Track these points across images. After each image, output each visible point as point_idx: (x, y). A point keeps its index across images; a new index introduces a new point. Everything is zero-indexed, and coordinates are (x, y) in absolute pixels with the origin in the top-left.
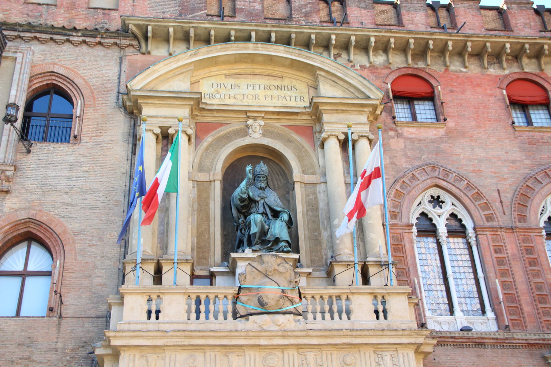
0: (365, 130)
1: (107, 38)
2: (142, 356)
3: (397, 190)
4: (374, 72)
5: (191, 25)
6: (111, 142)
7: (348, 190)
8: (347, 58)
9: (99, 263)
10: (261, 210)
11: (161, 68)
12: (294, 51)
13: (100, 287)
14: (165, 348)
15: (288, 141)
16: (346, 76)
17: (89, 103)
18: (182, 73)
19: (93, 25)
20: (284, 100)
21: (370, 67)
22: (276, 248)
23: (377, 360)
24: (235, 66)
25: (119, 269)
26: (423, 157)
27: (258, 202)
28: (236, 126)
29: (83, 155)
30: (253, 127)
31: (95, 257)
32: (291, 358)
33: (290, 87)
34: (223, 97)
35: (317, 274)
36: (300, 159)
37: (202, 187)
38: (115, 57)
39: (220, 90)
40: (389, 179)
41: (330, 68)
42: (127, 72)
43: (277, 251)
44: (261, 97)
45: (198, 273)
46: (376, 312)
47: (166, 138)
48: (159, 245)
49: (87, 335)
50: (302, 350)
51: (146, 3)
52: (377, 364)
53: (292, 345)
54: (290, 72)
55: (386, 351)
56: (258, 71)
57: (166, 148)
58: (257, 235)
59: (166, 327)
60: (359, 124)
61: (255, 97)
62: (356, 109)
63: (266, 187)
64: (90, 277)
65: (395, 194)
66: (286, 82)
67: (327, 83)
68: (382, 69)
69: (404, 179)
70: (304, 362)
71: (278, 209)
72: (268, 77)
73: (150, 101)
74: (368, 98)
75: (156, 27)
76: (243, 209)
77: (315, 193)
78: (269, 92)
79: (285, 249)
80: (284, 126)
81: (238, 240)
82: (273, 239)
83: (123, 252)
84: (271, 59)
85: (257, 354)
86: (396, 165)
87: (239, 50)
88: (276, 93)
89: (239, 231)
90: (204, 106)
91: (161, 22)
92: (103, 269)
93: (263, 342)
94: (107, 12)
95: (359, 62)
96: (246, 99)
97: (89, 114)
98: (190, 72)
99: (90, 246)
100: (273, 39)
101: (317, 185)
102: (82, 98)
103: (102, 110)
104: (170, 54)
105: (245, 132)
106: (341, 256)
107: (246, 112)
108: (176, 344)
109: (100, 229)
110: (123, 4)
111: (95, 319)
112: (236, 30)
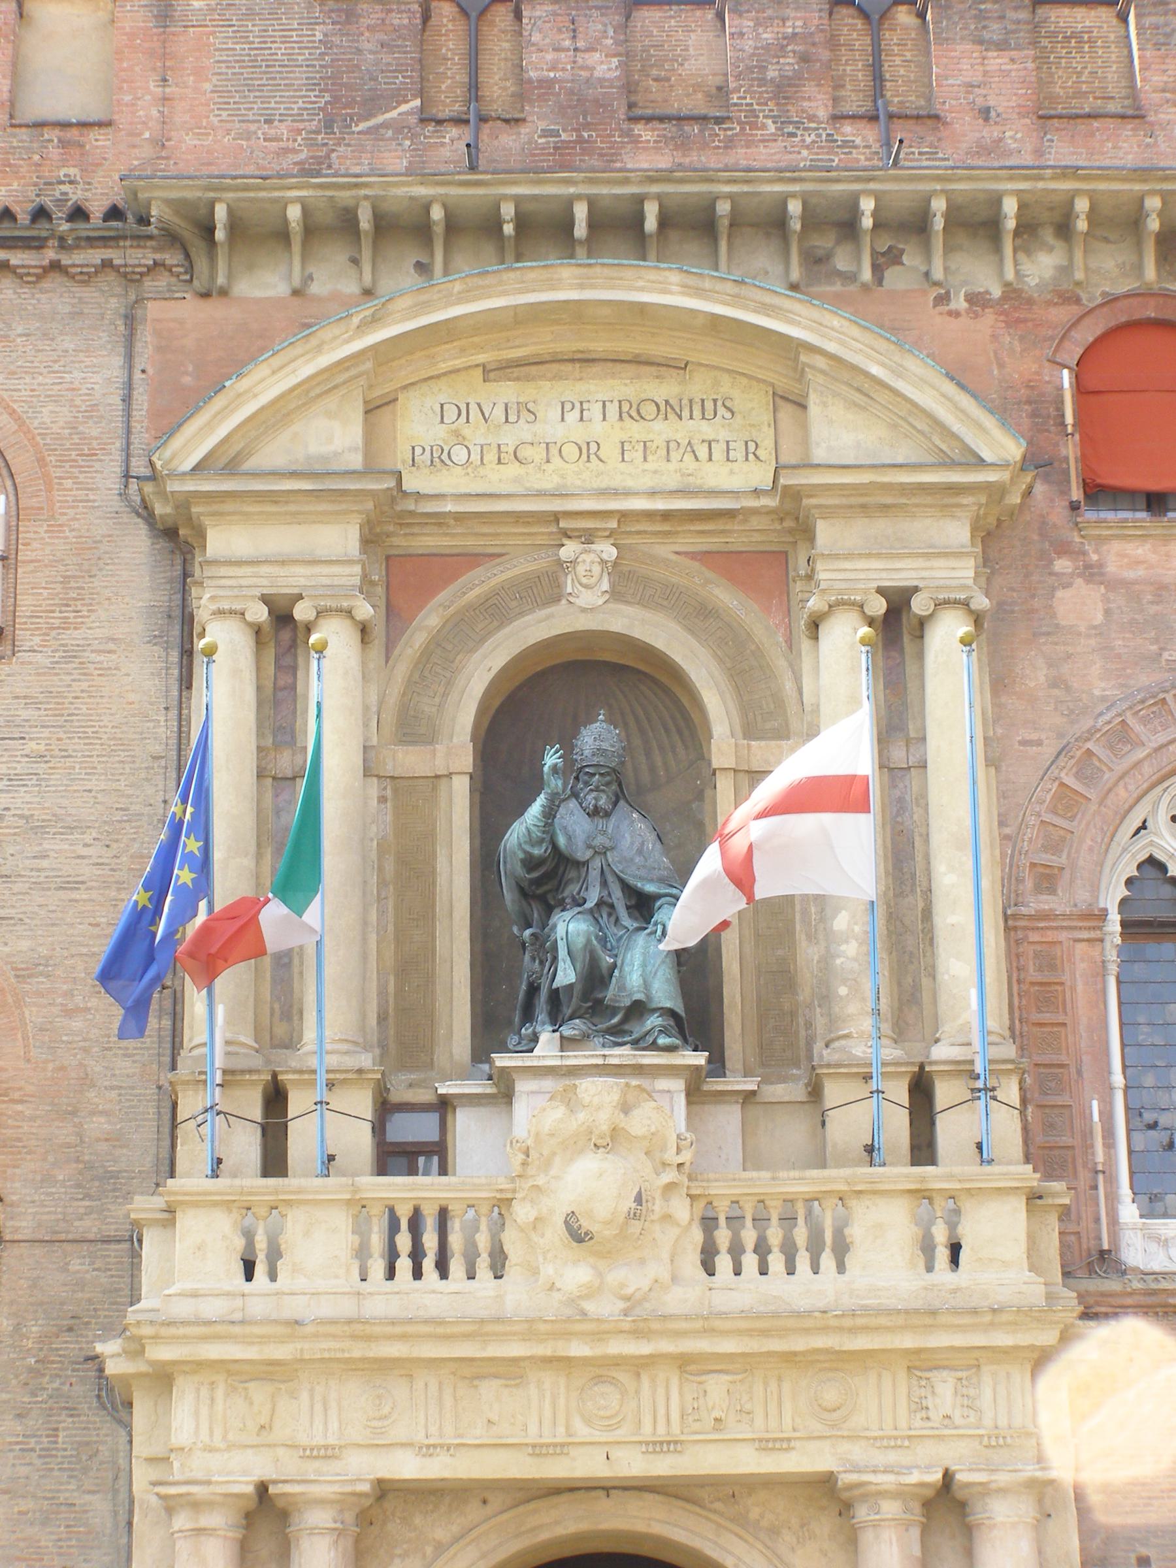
0: (962, 573)
1: (78, 247)
2: (235, 1389)
3: (1062, 784)
4: (1019, 321)
5: (363, 192)
6: (111, 646)
7: (897, 793)
8: (923, 268)
9: (97, 1069)
12: (719, 286)
13: (103, 1147)
15: (699, 615)
16: (899, 376)
17: (34, 502)
18: (335, 387)
19: (31, 193)
20: (688, 457)
21: (1005, 298)
22: (638, 1030)
25: (159, 1088)
26: (1166, 655)
29: (28, 700)
30: (581, 569)
31: (85, 1050)
33: (709, 405)
34: (476, 457)
35: (777, 1091)
38: (109, 315)
39: (467, 431)
40: (1039, 743)
41: (842, 343)
42: (150, 371)
43: (635, 1043)
44: (610, 451)
46: (928, 1248)
47: (283, 632)
48: (277, 1006)
49: (80, 1295)
51: (207, 86)
52: (913, 1406)
57: (287, 661)
60: (940, 559)
63: (615, 804)
64: (74, 1113)
65: (1058, 798)
66: (698, 387)
67: (836, 395)
68: (1049, 303)
69: (1089, 745)
71: (650, 888)
72: (632, 369)
73: (228, 507)
78: (636, 430)
79: (663, 1041)
80: (686, 554)
83: (169, 1033)
86: (1068, 689)
87: (528, 291)
88: (661, 430)
89: (527, 957)
90: (410, 506)
91: (259, 188)
92: (112, 1088)
94: (73, 134)
95: (965, 283)
96: (556, 460)
97: (35, 545)
98: (362, 381)
99: (69, 1013)
102: (9, 483)
103: (76, 525)
107: (556, 517)
109: (94, 954)
110: (127, 98)
111: (99, 1246)
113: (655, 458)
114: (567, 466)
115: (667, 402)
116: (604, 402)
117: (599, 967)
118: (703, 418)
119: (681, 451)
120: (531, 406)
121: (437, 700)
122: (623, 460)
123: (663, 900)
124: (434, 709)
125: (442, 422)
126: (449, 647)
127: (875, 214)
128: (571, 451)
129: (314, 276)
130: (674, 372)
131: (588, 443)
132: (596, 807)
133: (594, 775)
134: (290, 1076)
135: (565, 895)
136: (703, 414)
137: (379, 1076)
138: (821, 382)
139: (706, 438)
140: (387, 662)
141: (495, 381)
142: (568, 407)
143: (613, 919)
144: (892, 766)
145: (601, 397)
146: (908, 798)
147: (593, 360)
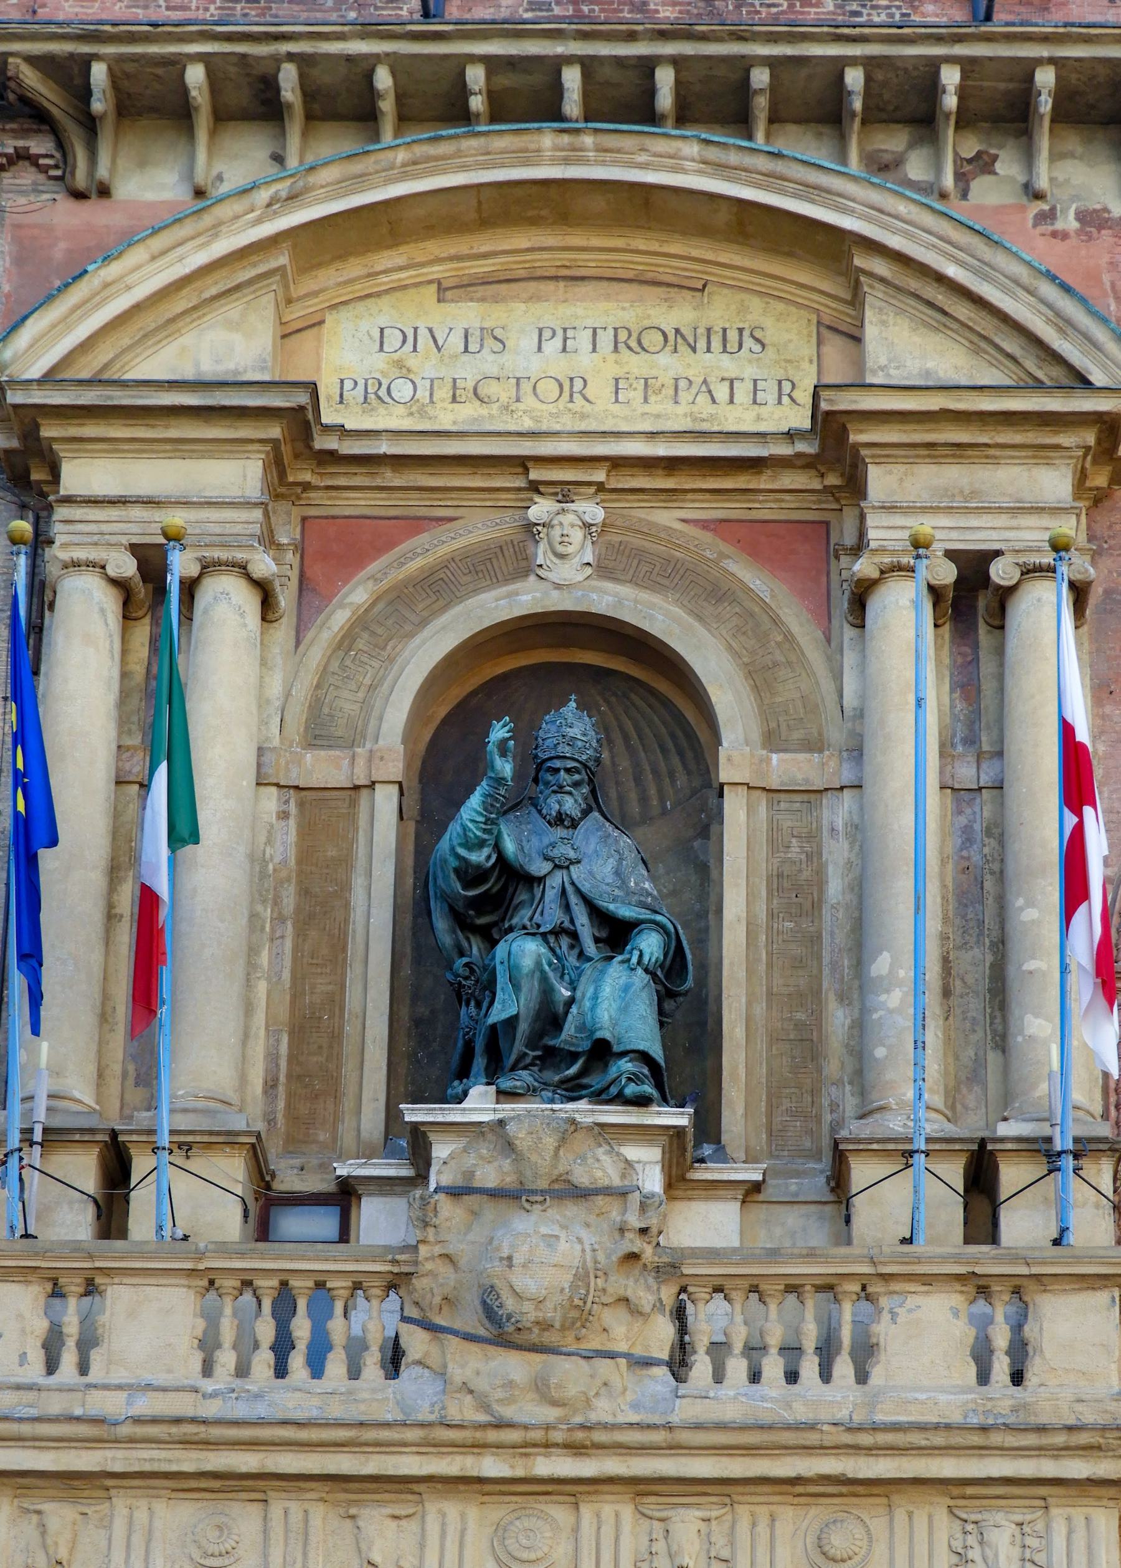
10: (552, 915)
11: (141, 274)
14: (109, 1482)
15: (710, 594)
20: (703, 399)
22: (596, 1081)
23: (958, 1545)
24: (484, 243)
27: (541, 880)
28: (479, 527)
30: (556, 532)
32: (608, 1531)
33: (733, 336)
34: (423, 394)
36: (760, 677)
37: (324, 813)
39: (412, 362)
45: (288, 1181)
50: (652, 1499)
53: (611, 1480)
54: (737, 260)
55: (1000, 1508)
56: (590, 263)
58: (523, 1027)
59: (112, 1404)
61: (571, 387)
62: (1018, 438)
63: (586, 813)
66: (719, 311)
70: (660, 1546)
71: (626, 912)
72: (635, 287)
74: (1083, 382)
75: (130, 67)
76: (480, 914)
77: (812, 837)
78: (635, 364)
79: (631, 1090)
81: (460, 1044)
82: (586, 1045)
84: (647, 203)
85: (473, 1512)
88: (667, 365)
93: (492, 1466)
96: (529, 401)
100: (665, 100)
101: (826, 799)
104: (199, 193)
105: (515, 557)
106: (888, 1115)
108: (147, 1467)
112: (491, 63)
113: (659, 397)
114: (544, 407)
115: (677, 331)
116: (595, 330)
117: (552, 1002)
118: (725, 351)
119: (694, 390)
120: (498, 333)
121: (361, 695)
122: (617, 401)
123: (643, 926)
124: (356, 707)
125: (381, 349)
126: (380, 631)
127: (963, 93)
128: (549, 389)
129: (225, 176)
130: (688, 294)
131: (571, 379)
132: (559, 813)
133: (557, 770)
134: (135, 1138)
135: (514, 921)
136: (725, 346)
137: (253, 1140)
138: (880, 295)
139: (726, 375)
140: (298, 643)
141: (452, 301)
142: (547, 334)
143: (576, 951)
144: (956, 786)
145: (590, 323)
146: (977, 827)
147: (583, 278)
